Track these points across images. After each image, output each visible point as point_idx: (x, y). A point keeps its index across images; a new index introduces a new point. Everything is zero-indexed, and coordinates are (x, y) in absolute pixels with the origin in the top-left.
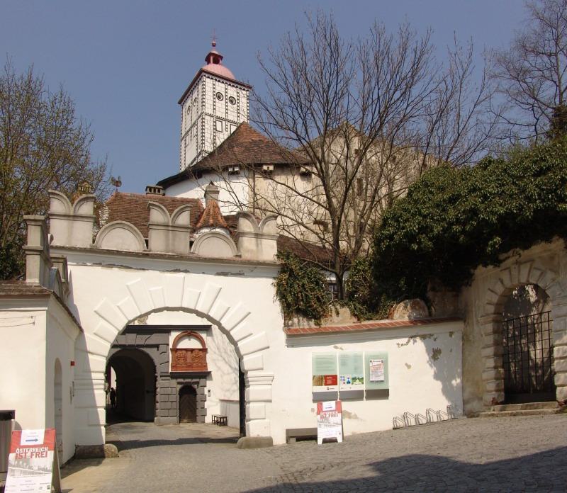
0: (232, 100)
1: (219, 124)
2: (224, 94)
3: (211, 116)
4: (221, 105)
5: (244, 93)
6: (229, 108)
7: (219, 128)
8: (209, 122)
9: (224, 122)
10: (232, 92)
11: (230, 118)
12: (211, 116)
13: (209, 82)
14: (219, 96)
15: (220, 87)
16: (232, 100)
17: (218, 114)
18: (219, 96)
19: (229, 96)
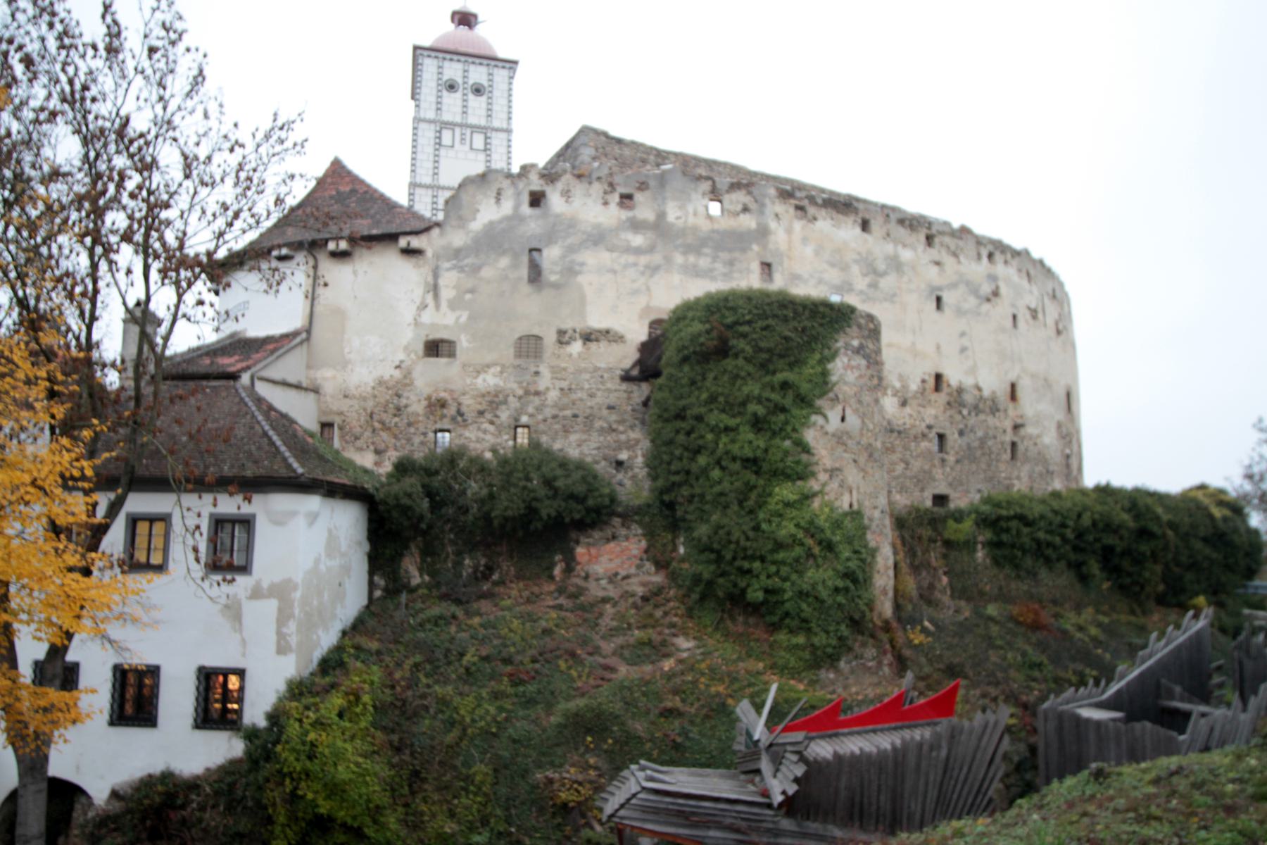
0: (478, 91)
1: (447, 137)
2: (460, 81)
4: (452, 103)
5: (500, 75)
9: (458, 130)
11: (472, 120)
13: (429, 66)
14: (452, 87)
15: (453, 70)
17: (447, 117)
19: (471, 82)
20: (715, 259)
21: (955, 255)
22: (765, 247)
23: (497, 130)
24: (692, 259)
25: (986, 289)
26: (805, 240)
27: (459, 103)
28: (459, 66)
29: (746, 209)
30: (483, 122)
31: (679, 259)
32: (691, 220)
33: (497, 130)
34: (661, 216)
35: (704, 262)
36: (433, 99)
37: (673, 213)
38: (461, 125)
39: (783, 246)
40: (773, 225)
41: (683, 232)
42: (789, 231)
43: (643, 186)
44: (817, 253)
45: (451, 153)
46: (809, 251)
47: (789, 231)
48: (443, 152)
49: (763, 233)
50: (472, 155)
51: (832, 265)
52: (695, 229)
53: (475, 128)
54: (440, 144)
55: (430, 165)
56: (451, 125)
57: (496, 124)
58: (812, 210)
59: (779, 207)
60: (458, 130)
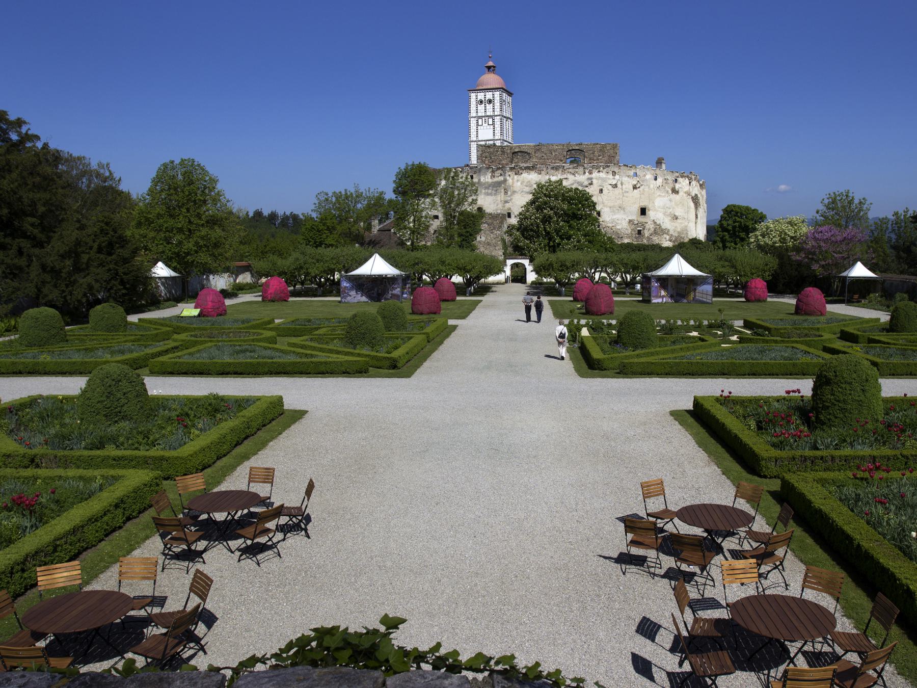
0: (490, 101)
1: (480, 121)
3: (475, 117)
4: (481, 108)
5: (497, 94)
6: (487, 108)
7: (480, 123)
8: (473, 122)
9: (483, 118)
10: (489, 95)
11: (488, 114)
12: (475, 117)
13: (473, 95)
14: (481, 102)
15: (481, 96)
16: (490, 101)
17: (480, 114)
18: (481, 102)
20: (492, 190)
21: (573, 174)
22: (505, 185)
23: (496, 116)
24: (487, 191)
25: (586, 183)
26: (518, 181)
27: (484, 108)
28: (483, 94)
29: (501, 175)
30: (492, 114)
31: (483, 191)
32: (487, 180)
33: (496, 116)
34: (479, 180)
35: (490, 191)
36: (475, 108)
37: (482, 179)
38: (484, 117)
39: (511, 184)
40: (508, 178)
41: (485, 183)
42: (513, 179)
43: (475, 173)
44: (522, 184)
45: (482, 127)
46: (519, 183)
47: (513, 179)
48: (479, 127)
49: (505, 180)
50: (488, 127)
51: (527, 186)
52: (488, 182)
53: (489, 117)
54: (478, 125)
55: (475, 133)
56: (481, 117)
57: (496, 114)
58: (521, 172)
59: (509, 173)
60: (483, 118)
